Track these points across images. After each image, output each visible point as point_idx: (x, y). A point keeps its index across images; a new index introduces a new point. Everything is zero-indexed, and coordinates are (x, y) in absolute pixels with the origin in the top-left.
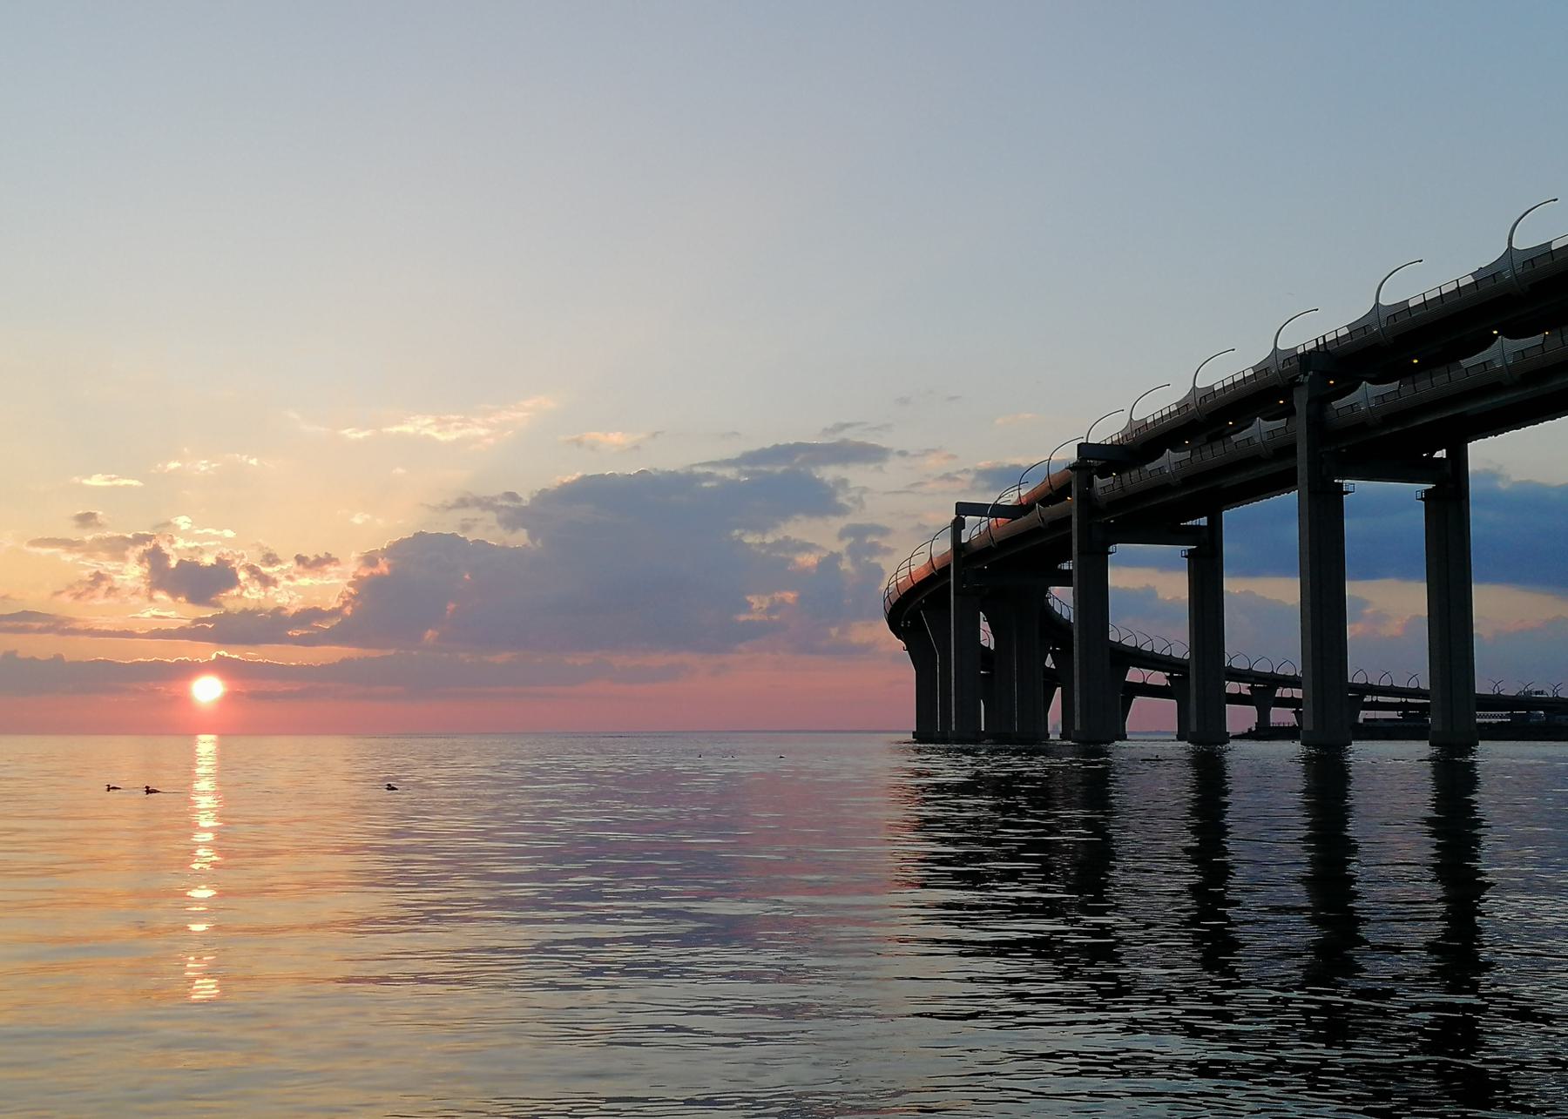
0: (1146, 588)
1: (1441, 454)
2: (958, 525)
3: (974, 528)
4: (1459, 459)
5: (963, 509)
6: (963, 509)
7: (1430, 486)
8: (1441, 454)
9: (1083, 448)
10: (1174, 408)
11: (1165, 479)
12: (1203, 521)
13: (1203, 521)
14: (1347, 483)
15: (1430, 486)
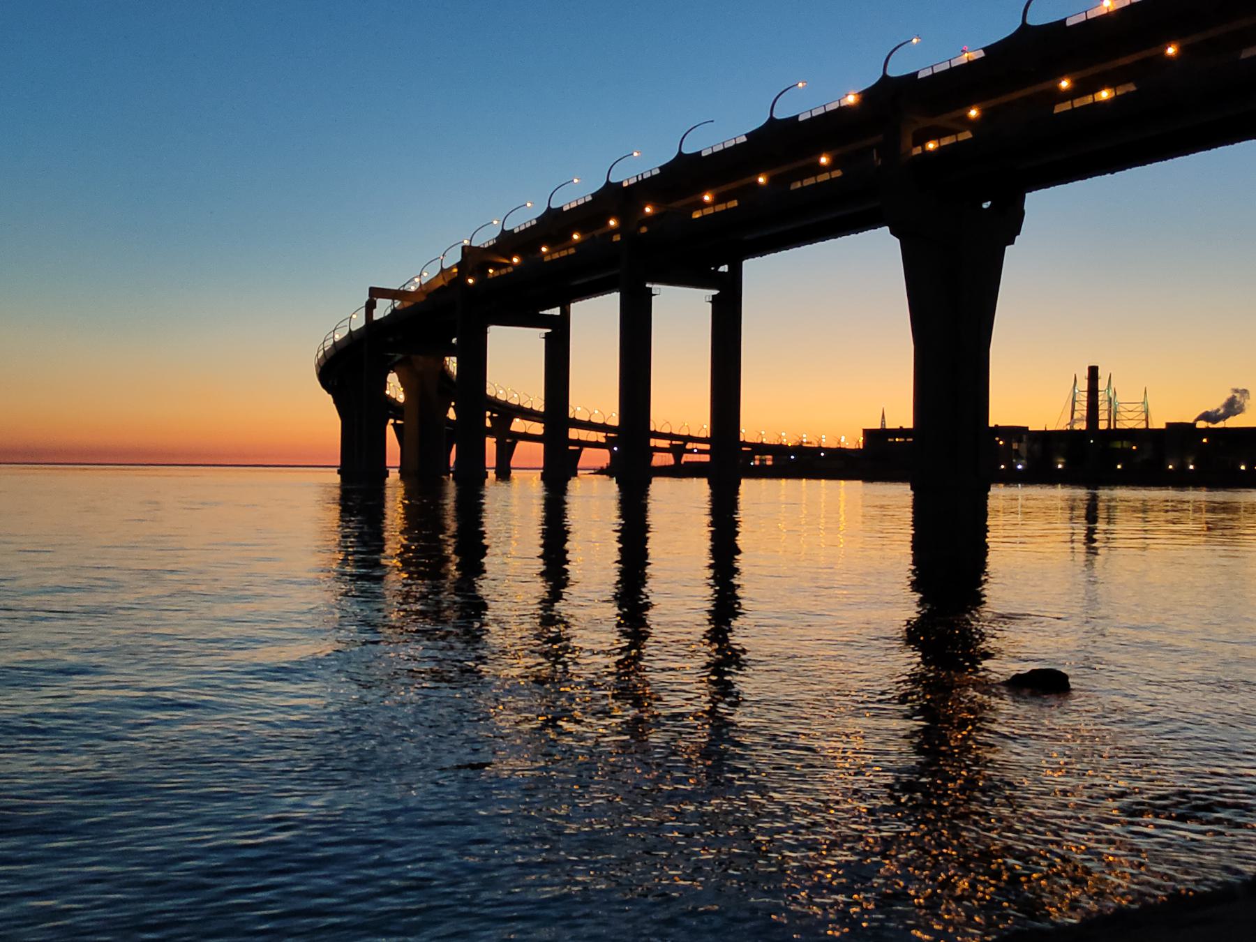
0: (512, 362)
1: (724, 268)
2: (370, 306)
3: (383, 309)
4: (736, 274)
5: (376, 293)
6: (376, 293)
7: (716, 292)
8: (724, 268)
9: (468, 251)
10: (534, 222)
11: (527, 276)
12: (556, 311)
13: (556, 311)
14: (656, 288)
15: (716, 292)
